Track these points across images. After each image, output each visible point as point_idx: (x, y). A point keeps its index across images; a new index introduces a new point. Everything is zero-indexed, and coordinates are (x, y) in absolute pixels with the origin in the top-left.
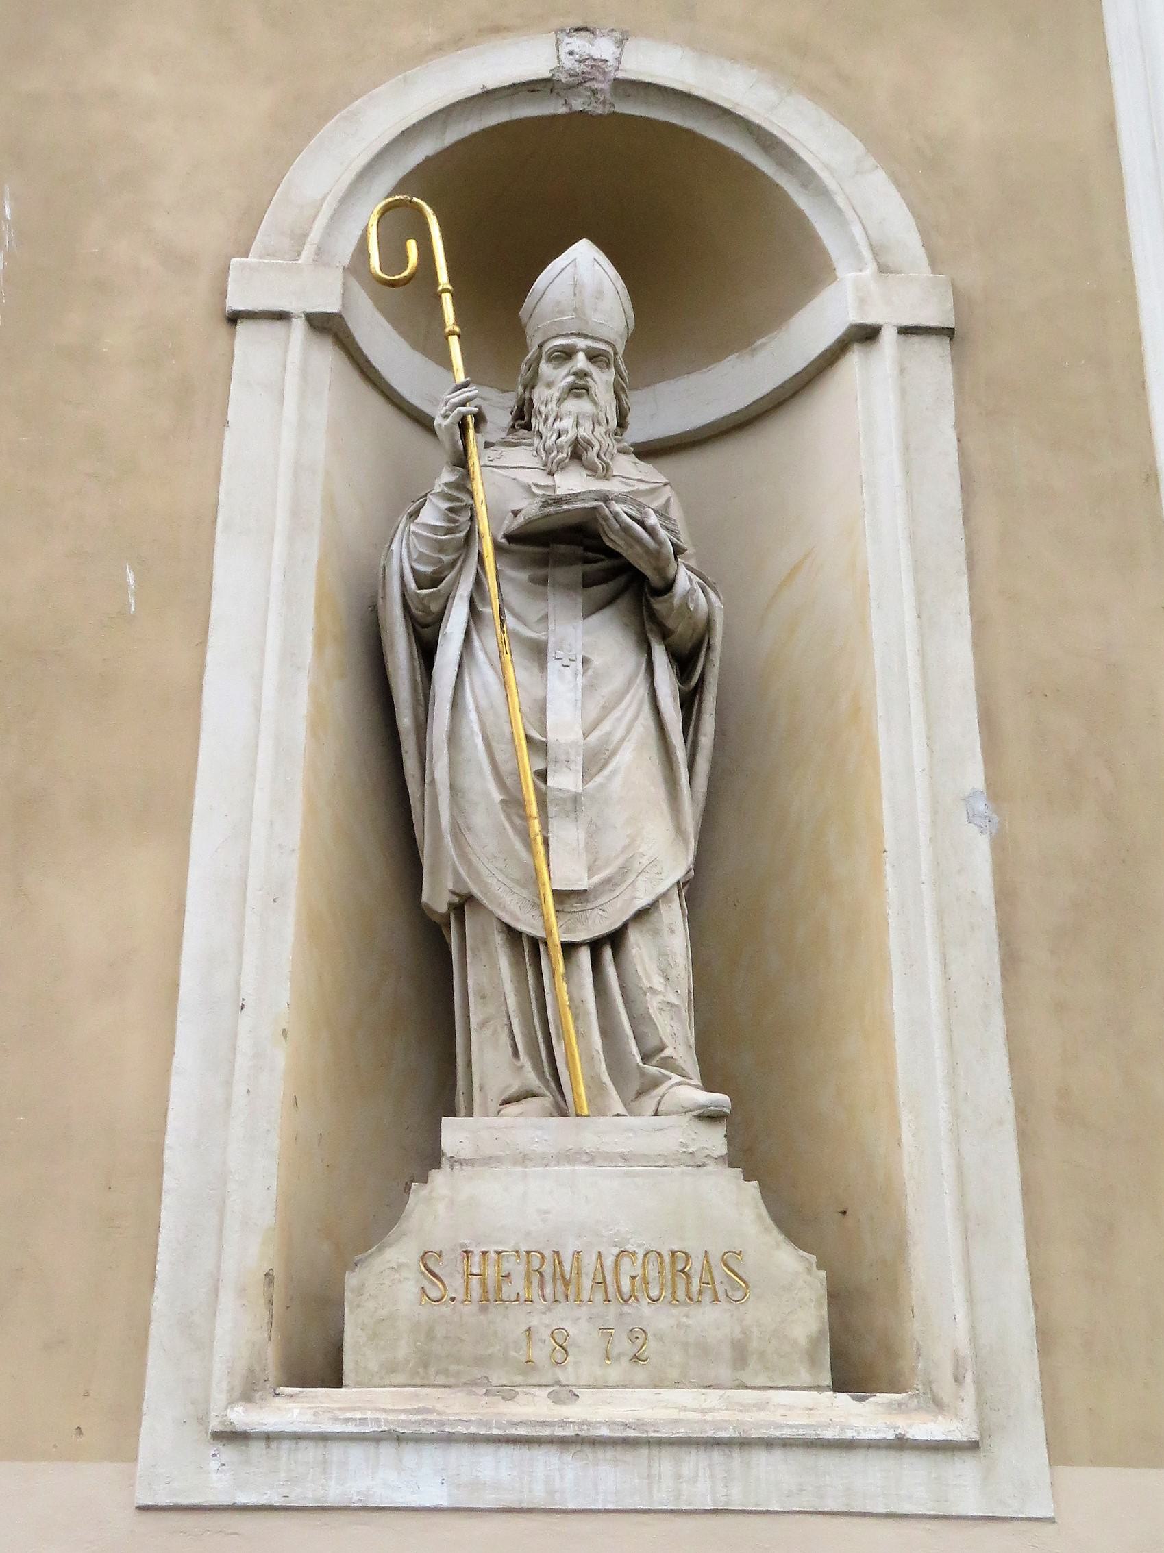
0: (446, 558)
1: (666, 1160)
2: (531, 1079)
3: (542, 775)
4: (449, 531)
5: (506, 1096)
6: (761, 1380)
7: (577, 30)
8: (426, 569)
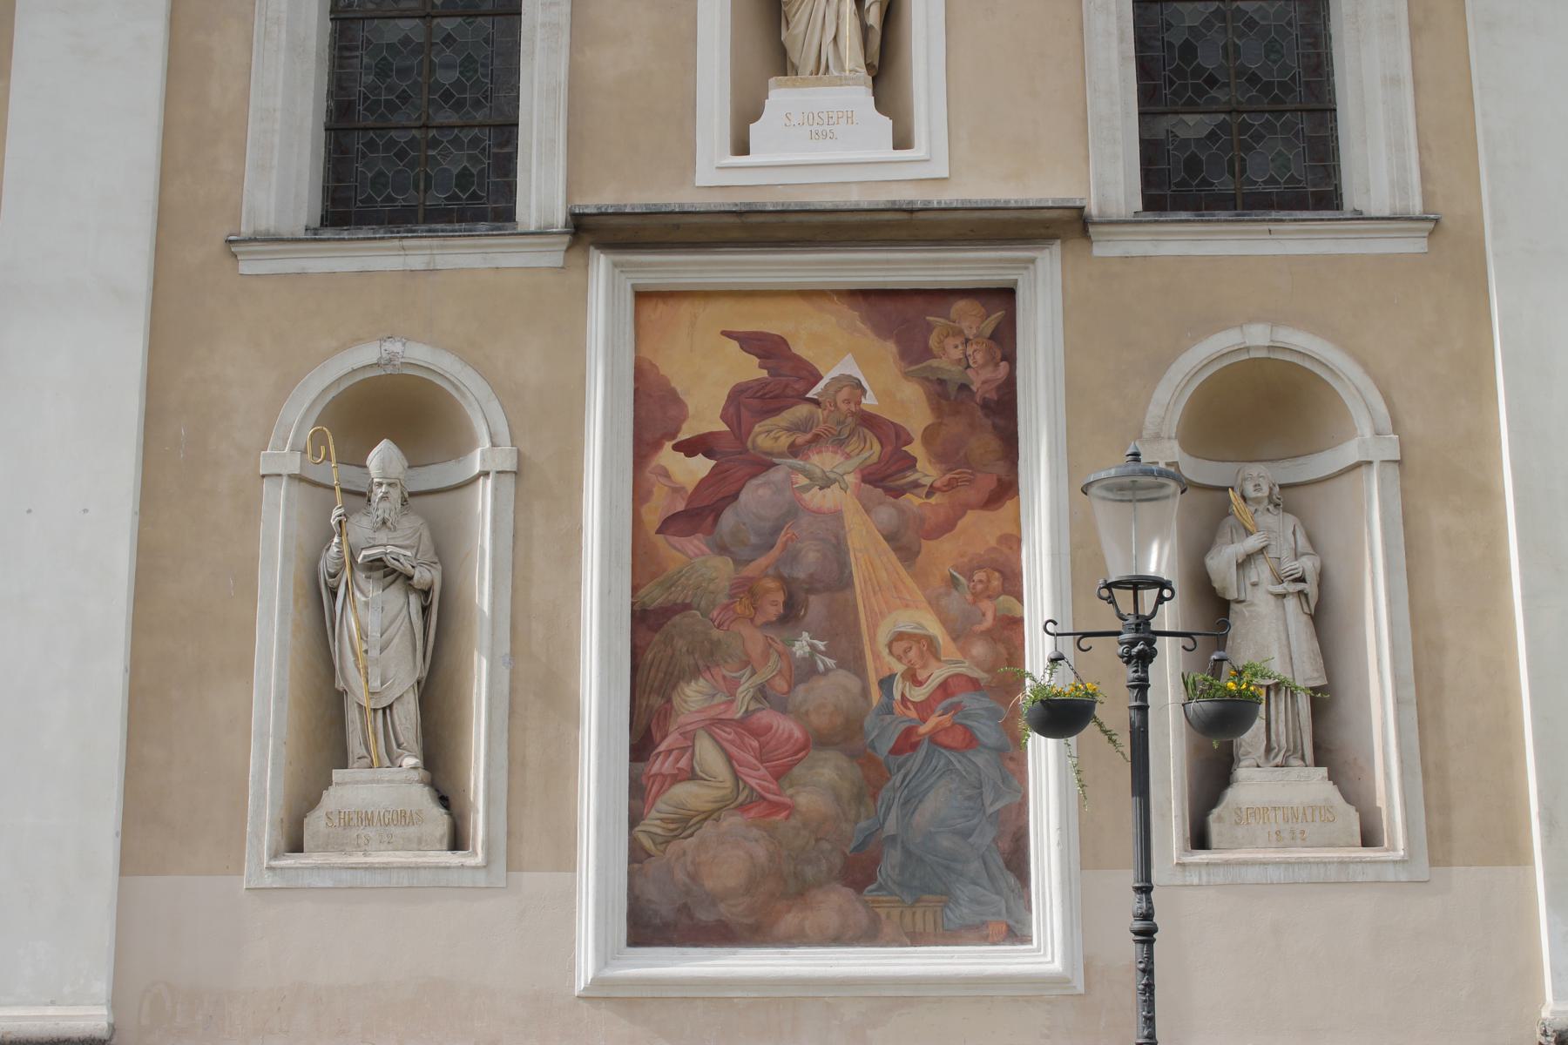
0: (338, 568)
1: (401, 782)
2: (366, 754)
3: (366, 652)
4: (338, 559)
5: (360, 756)
6: (425, 848)
7: (389, 338)
8: (332, 571)
